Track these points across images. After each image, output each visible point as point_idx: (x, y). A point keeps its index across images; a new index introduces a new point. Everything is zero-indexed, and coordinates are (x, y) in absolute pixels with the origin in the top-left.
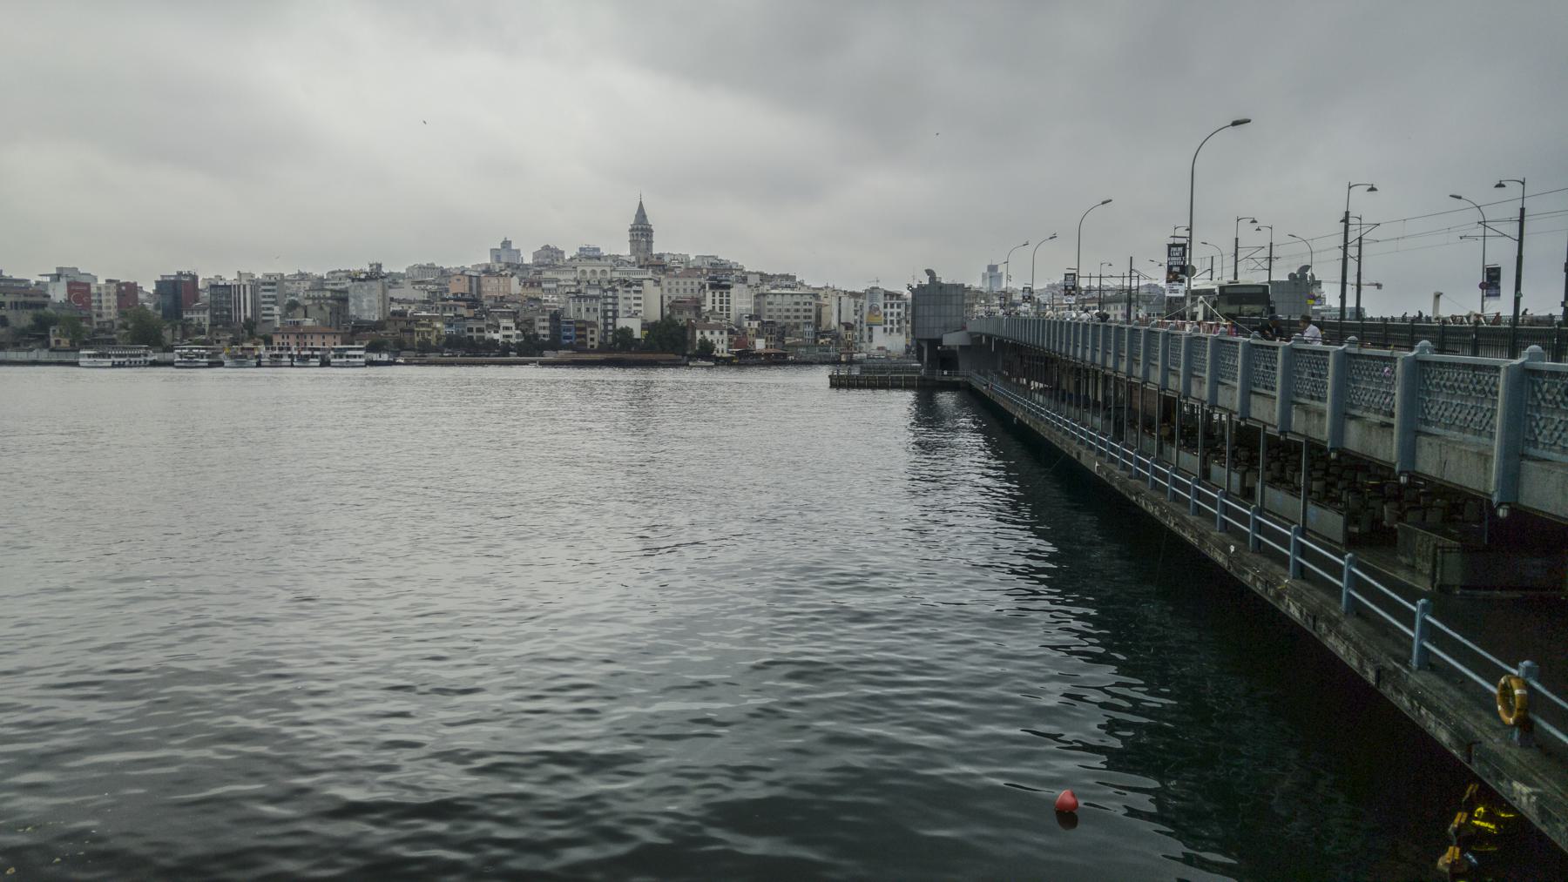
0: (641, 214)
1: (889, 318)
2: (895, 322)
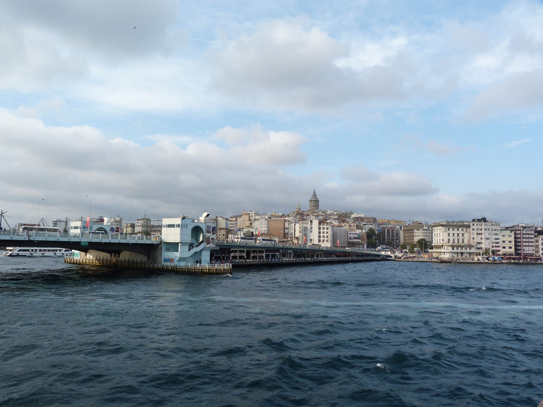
0: (315, 195)
1: (322, 235)
2: (325, 237)
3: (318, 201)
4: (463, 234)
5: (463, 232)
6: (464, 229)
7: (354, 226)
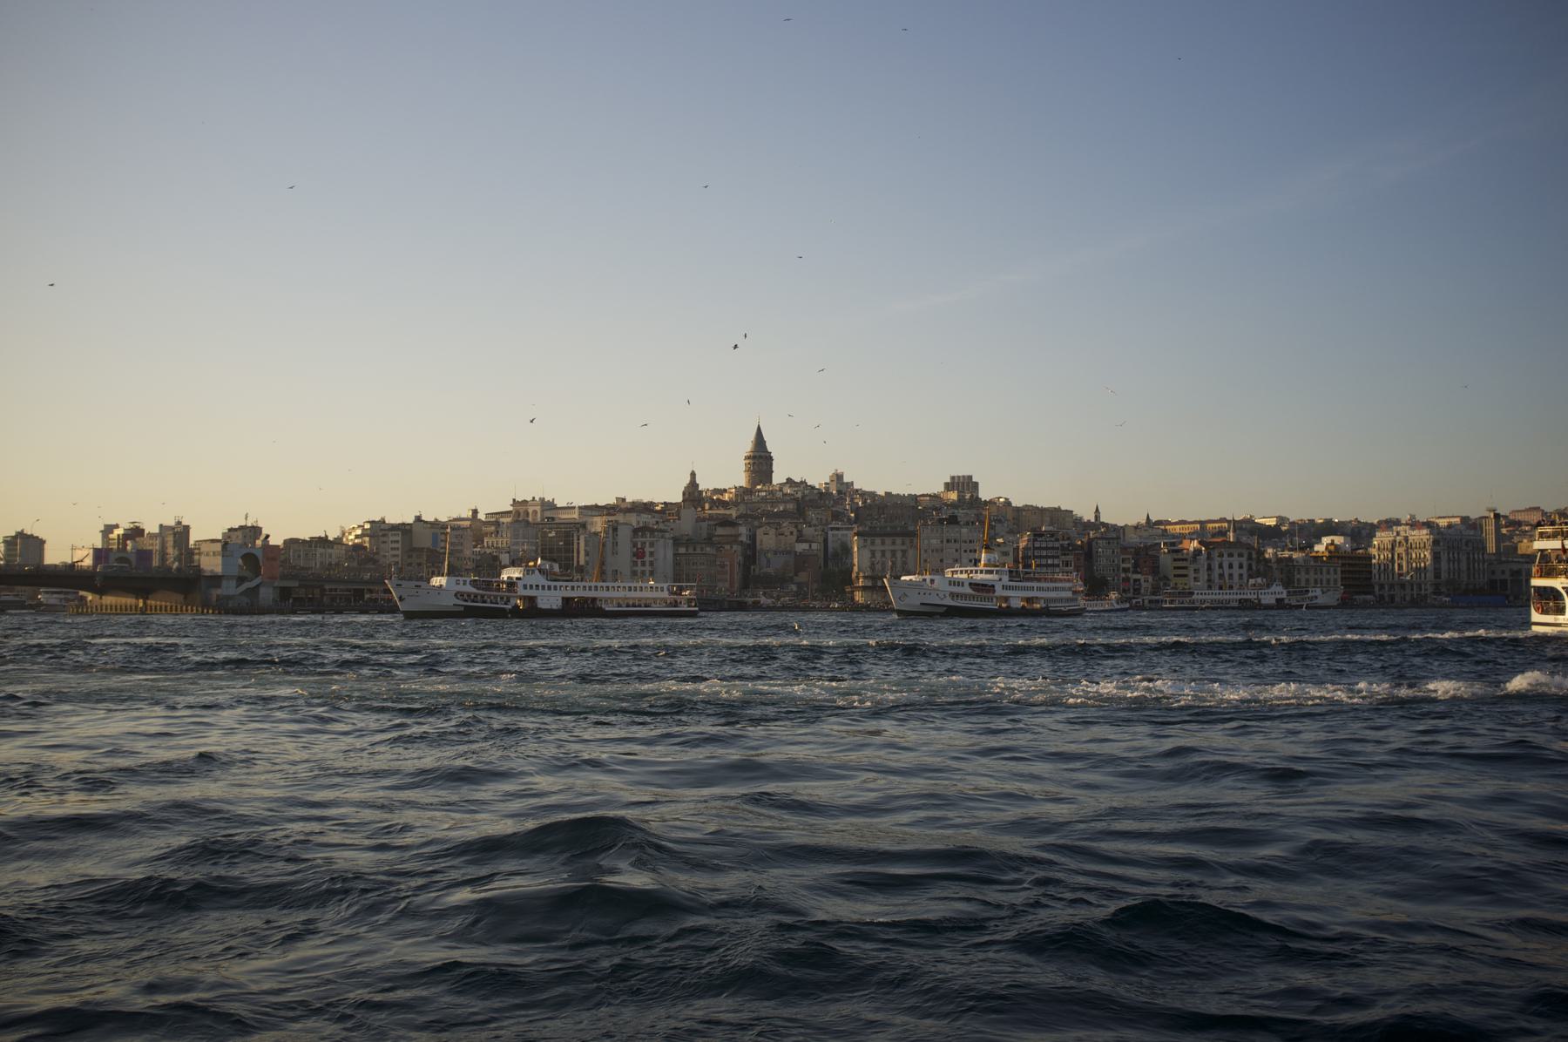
0: (760, 441)
3: (770, 459)
4: (904, 552)
5: (904, 548)
6: (907, 540)
7: (792, 533)
